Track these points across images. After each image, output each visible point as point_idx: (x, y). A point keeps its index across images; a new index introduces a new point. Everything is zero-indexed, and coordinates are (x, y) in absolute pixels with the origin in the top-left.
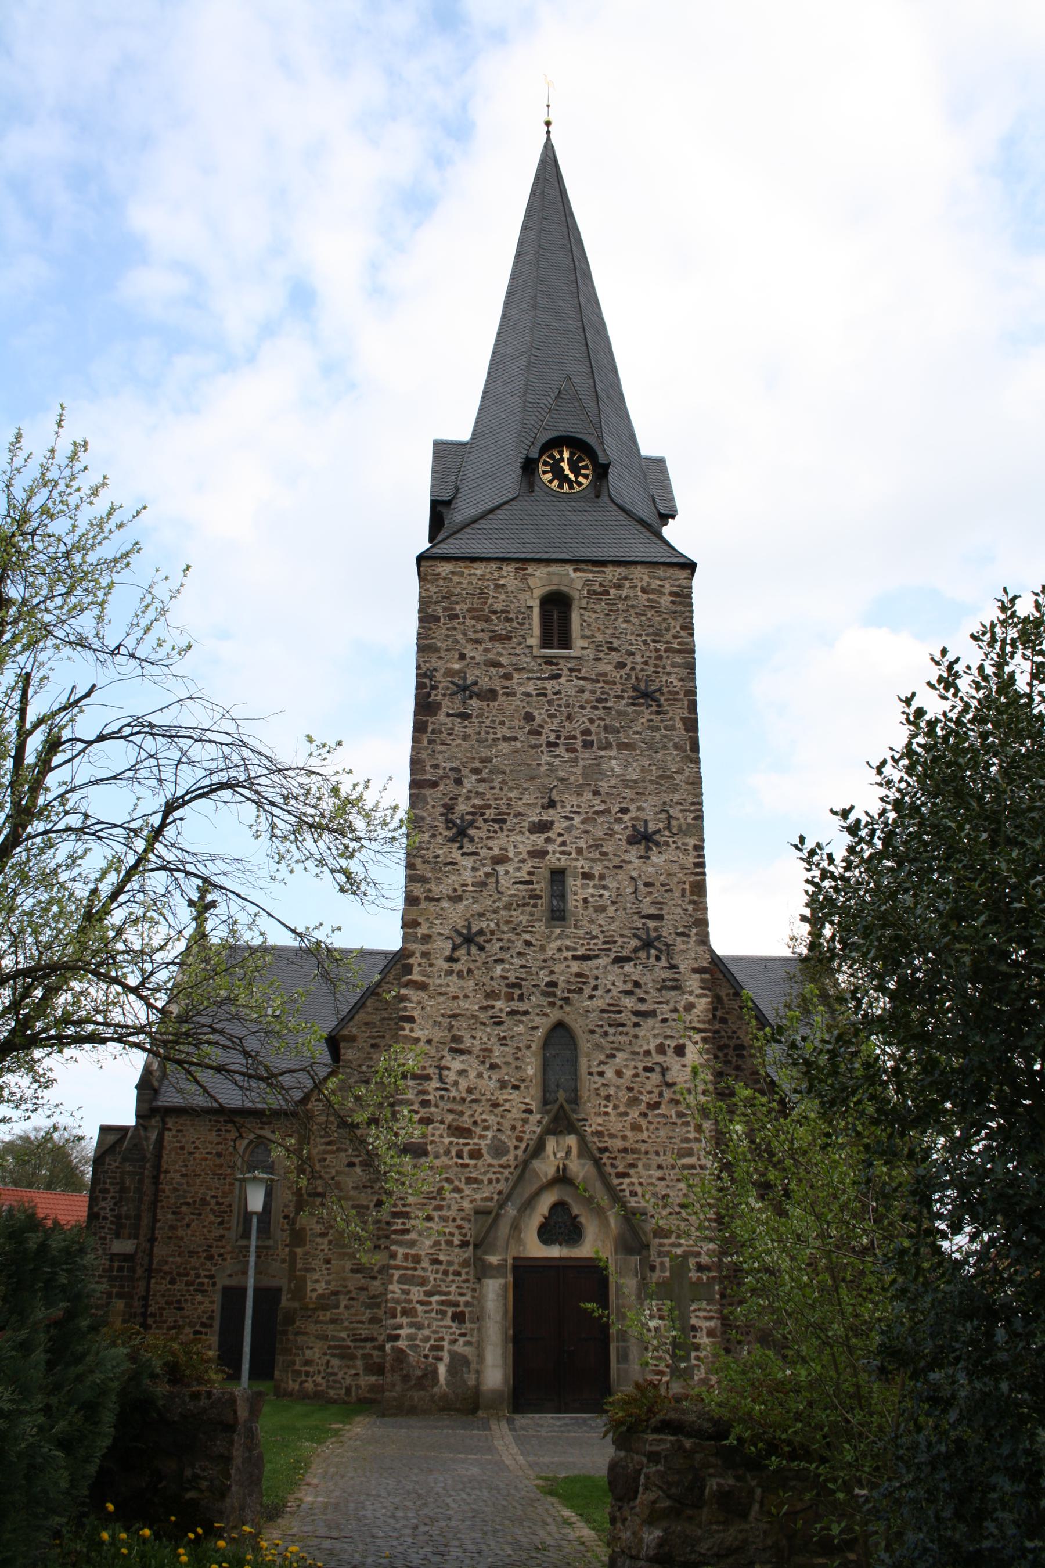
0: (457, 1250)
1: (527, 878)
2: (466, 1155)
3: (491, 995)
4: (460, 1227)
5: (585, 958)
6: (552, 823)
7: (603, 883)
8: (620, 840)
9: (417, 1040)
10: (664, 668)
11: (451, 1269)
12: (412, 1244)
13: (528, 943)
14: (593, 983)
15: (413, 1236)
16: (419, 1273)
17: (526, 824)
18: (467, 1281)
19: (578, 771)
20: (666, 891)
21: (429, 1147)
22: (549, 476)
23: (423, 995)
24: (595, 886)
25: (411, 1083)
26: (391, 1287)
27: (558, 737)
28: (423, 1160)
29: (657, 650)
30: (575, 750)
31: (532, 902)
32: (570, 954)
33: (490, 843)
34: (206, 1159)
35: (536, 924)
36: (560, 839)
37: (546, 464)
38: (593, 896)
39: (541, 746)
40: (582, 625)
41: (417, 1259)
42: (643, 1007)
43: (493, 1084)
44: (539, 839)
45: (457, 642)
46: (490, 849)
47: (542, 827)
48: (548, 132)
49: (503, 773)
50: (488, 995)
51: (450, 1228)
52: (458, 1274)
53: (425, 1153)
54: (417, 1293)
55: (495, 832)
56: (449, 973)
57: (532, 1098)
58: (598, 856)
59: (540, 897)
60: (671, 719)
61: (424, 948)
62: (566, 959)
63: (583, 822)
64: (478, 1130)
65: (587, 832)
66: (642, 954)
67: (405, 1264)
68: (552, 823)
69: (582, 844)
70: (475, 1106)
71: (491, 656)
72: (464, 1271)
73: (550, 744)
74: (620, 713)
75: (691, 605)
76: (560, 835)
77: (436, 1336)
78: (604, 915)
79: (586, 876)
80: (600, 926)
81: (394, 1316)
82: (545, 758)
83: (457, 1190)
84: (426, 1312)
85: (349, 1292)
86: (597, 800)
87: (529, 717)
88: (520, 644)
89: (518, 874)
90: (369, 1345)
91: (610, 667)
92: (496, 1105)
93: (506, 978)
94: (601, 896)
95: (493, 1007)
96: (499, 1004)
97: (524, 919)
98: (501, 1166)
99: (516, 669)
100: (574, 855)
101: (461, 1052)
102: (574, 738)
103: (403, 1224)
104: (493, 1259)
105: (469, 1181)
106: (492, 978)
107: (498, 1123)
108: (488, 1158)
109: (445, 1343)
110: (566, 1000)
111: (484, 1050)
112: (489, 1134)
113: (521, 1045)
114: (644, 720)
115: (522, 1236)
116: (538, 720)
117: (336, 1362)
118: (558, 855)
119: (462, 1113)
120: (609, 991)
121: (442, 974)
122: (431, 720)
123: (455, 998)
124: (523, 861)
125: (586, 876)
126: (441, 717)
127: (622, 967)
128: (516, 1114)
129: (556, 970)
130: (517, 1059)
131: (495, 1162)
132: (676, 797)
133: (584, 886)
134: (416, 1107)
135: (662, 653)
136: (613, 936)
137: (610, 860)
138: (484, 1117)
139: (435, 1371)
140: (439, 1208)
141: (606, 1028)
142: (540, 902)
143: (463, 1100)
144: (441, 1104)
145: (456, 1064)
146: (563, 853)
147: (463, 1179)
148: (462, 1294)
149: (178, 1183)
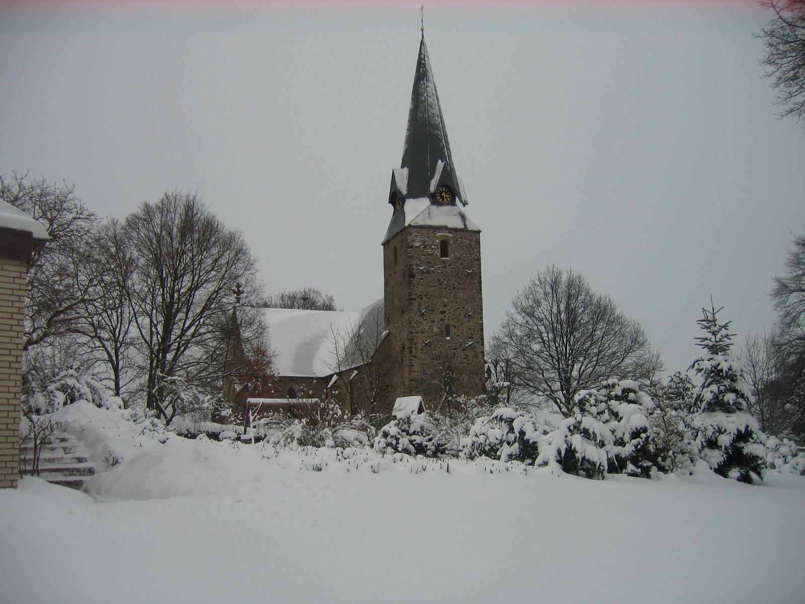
5: (455, 349)
9: (415, 371)
13: (441, 345)
14: (457, 355)
19: (452, 296)
22: (439, 197)
23: (416, 359)
29: (471, 259)
33: (430, 317)
42: (468, 362)
44: (442, 316)
47: (443, 312)
48: (423, 34)
50: (432, 359)
56: (422, 353)
58: (457, 321)
59: (443, 332)
63: (453, 311)
65: (454, 314)
66: (469, 348)
69: (453, 317)
71: (428, 260)
73: (445, 288)
74: (462, 278)
79: (455, 326)
87: (439, 280)
96: (434, 361)
101: (426, 374)
123: (424, 360)
124: (439, 322)
125: (455, 326)
126: (416, 278)
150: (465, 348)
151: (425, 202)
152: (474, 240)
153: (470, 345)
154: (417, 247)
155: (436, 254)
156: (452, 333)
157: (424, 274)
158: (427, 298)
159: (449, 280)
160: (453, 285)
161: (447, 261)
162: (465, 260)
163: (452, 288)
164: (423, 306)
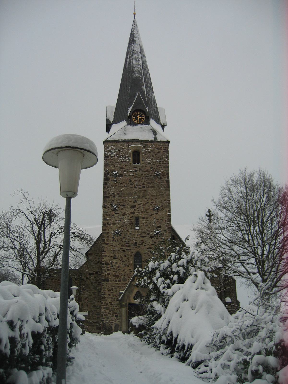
0: (116, 302)
1: (130, 219)
2: (117, 281)
3: (122, 246)
4: (116, 297)
6: (136, 206)
7: (147, 219)
8: (151, 209)
9: (106, 256)
10: (162, 168)
11: (115, 306)
12: (106, 300)
13: (131, 234)
14: (145, 242)
15: (106, 299)
16: (108, 307)
17: (130, 206)
18: (118, 308)
19: (142, 193)
20: (162, 221)
21: (109, 279)
24: (145, 220)
25: (105, 265)
26: (102, 310)
27: (137, 186)
28: (108, 282)
29: (160, 164)
30: (140, 188)
31: (131, 224)
32: (140, 236)
34: (55, 281)
35: (132, 229)
36: (138, 210)
37: (134, 116)
38: (145, 222)
39: (133, 188)
40: (142, 158)
41: (107, 304)
43: (123, 265)
44: (132, 210)
45: (113, 163)
46: (122, 212)
47: (133, 207)
49: (124, 194)
51: (115, 297)
52: (116, 307)
53: (109, 281)
54: (107, 311)
55: (123, 208)
56: (113, 241)
57: (132, 268)
59: (133, 223)
60: (163, 180)
61: (108, 235)
62: (139, 237)
63: (143, 205)
64: (120, 275)
66: (156, 236)
67: (105, 305)
68: (136, 206)
69: (142, 210)
70: (119, 270)
71: (121, 166)
72: (117, 306)
73: (135, 187)
75: (168, 152)
76: (138, 209)
77: (112, 320)
78: (147, 227)
79: (144, 218)
80: (147, 229)
81: (103, 316)
82: (134, 190)
83: (115, 289)
84: (110, 315)
85: (93, 312)
86: (146, 200)
87: (130, 181)
88: (128, 163)
89: (128, 218)
90: (97, 323)
91: (149, 168)
92: (124, 270)
93: (126, 242)
94: (147, 222)
95: (123, 248)
96: (124, 247)
97: (130, 228)
98: (125, 283)
99: (127, 169)
100: (141, 213)
101: (116, 258)
102: (140, 185)
103: (104, 296)
104: (124, 304)
105: (118, 287)
106: (123, 242)
107: (124, 274)
108: (122, 282)
109: (114, 322)
110: (139, 246)
111: (121, 258)
112: (123, 276)
113: (129, 257)
114: (156, 181)
115: (130, 298)
116: (132, 181)
117: (90, 327)
118: (137, 213)
119: (116, 272)
120: (149, 244)
121: (111, 241)
122: (108, 182)
123: (114, 246)
125: (144, 218)
126: (110, 181)
127: (151, 239)
128: (128, 272)
129: (137, 240)
130: (128, 260)
131: (123, 282)
132: (164, 199)
133: (143, 220)
134: (106, 271)
135: (161, 164)
136: (149, 232)
137: (149, 214)
138: (121, 273)
139: (112, 328)
140: (112, 293)
141: (148, 253)
142: (133, 224)
143: (117, 269)
144: (112, 270)
145: (115, 261)
146: (138, 213)
147: (117, 287)
148: (117, 311)
149: (49, 287)
150: (153, 235)
151: (124, 123)
152: (163, 148)
153: (158, 233)
154: (112, 157)
155: (129, 161)
156: (140, 224)
157: (118, 178)
158: (119, 196)
159: (139, 181)
160: (143, 184)
161: (139, 166)
162: (154, 165)
163: (142, 187)
164: (115, 202)
